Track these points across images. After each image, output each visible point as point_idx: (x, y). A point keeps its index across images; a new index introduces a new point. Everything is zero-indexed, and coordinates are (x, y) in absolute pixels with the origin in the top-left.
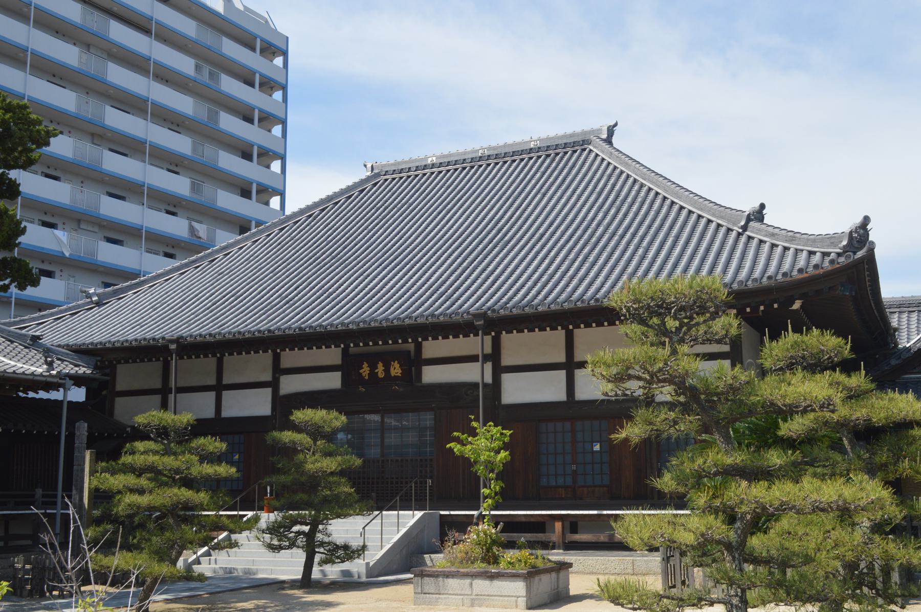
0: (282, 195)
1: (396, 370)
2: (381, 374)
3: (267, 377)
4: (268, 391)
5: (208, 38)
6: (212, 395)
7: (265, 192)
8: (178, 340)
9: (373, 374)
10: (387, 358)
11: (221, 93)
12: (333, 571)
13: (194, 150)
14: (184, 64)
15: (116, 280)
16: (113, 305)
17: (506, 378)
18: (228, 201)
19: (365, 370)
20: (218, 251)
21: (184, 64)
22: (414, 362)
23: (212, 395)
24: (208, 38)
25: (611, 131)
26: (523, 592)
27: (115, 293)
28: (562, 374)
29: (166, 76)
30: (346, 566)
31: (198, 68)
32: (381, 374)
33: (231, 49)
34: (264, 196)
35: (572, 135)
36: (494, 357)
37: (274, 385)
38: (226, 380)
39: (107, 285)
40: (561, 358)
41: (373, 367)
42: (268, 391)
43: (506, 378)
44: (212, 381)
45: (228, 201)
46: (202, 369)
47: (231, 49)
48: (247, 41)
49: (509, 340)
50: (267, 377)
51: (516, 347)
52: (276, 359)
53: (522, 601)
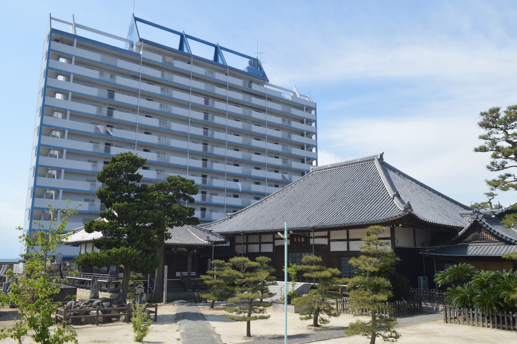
0: (317, 160)
1: (303, 240)
2: (299, 241)
3: (271, 240)
4: (272, 244)
5: (286, 109)
6: (258, 245)
7: (310, 160)
8: (243, 232)
9: (297, 241)
10: (301, 237)
11: (292, 128)
12: (268, 300)
13: (283, 148)
14: (278, 120)
15: (235, 210)
16: (234, 218)
17: (331, 243)
18: (296, 165)
19: (295, 240)
20: (272, 196)
21: (278, 120)
22: (308, 238)
23: (258, 245)
24: (286, 109)
25: (382, 155)
26: (294, 309)
27: (235, 214)
28: (350, 242)
29: (272, 126)
30: (272, 298)
31: (283, 120)
32: (299, 241)
33: (295, 112)
34: (310, 161)
35: (369, 157)
36: (328, 237)
37: (273, 243)
38: (262, 241)
39: (234, 211)
40: (346, 238)
41: (297, 239)
42: (272, 244)
43: (331, 243)
44: (258, 241)
45: (296, 165)
46: (256, 239)
47: (295, 112)
48: (300, 107)
49: (332, 232)
50: (271, 240)
51: (334, 235)
52: (274, 236)
53: (294, 311)
